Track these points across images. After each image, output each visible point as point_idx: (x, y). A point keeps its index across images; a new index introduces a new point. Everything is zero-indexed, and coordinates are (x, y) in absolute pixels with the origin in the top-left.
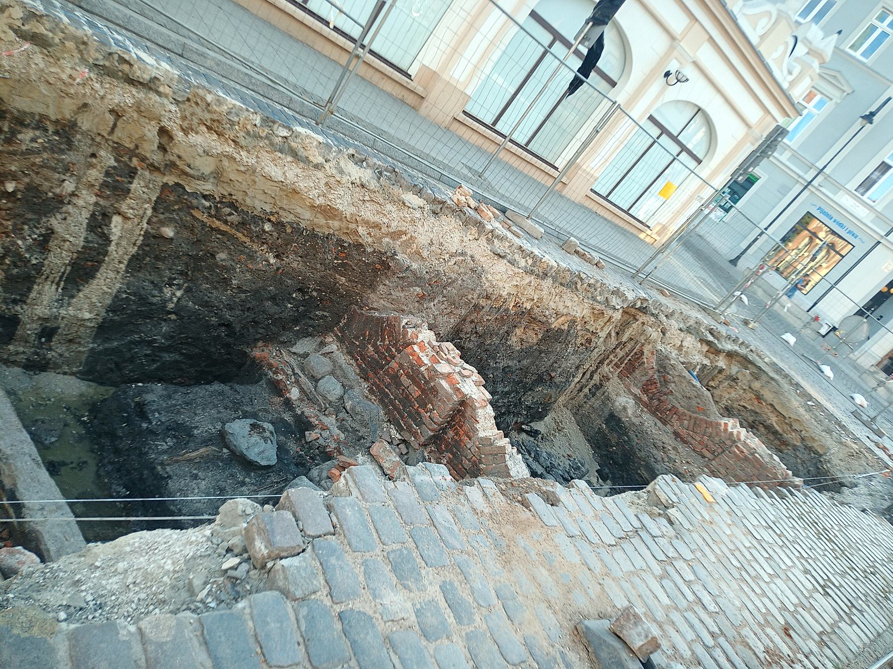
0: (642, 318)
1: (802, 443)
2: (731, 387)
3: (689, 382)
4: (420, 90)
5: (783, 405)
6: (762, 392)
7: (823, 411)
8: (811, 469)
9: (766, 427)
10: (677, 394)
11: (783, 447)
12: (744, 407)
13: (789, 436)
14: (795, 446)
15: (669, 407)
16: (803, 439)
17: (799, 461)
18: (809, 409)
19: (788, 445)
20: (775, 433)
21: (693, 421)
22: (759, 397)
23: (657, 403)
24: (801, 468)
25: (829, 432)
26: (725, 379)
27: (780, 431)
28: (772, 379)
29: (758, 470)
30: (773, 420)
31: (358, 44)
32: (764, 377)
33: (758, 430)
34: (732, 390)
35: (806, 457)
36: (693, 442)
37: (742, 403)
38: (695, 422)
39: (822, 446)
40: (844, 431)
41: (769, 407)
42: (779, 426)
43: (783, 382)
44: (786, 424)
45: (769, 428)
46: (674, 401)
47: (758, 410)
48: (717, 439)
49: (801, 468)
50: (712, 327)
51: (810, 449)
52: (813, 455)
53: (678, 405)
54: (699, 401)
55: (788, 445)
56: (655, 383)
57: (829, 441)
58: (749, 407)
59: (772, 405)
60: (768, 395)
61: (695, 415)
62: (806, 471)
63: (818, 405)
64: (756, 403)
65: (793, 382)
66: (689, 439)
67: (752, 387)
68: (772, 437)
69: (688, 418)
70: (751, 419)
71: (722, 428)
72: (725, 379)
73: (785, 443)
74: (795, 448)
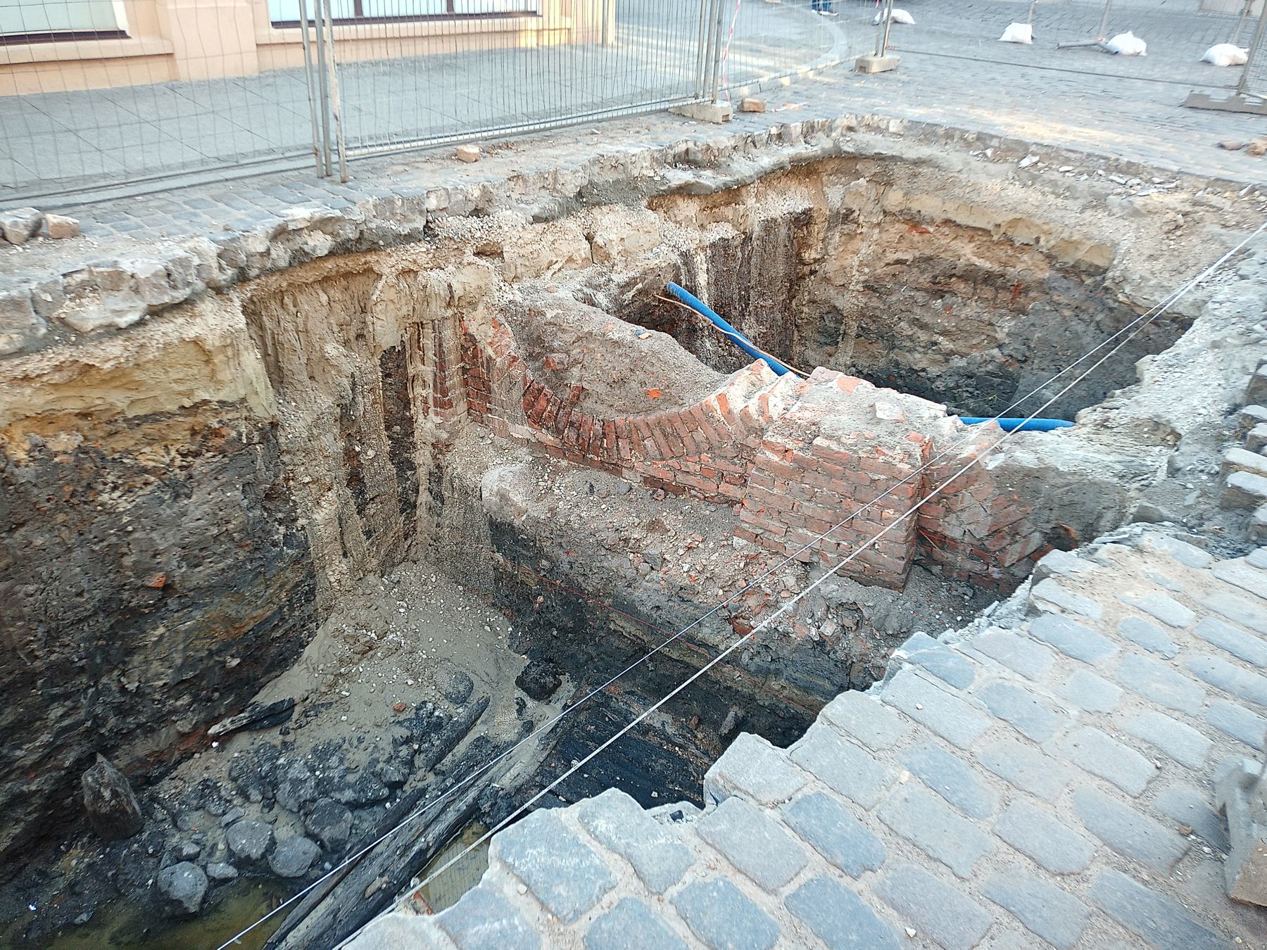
0: (387, 264)
1: (1052, 267)
2: (851, 236)
4: (152, 45)
5: (971, 207)
6: (915, 206)
7: (1067, 161)
8: (1099, 318)
11: (1022, 300)
12: (898, 262)
14: (1041, 283)
16: (1050, 257)
17: (1067, 313)
18: (1031, 178)
19: (1027, 290)
20: (988, 278)
21: (657, 432)
22: (915, 222)
23: (573, 435)
24: (1080, 328)
25: (1098, 202)
26: (829, 229)
27: (996, 268)
28: (918, 162)
29: (843, 477)
30: (968, 253)
31: (304, 24)
32: (899, 171)
34: (857, 244)
35: (1078, 293)
36: (691, 481)
37: (892, 257)
39: (1100, 247)
40: (1136, 175)
41: (946, 230)
42: (987, 259)
44: (998, 243)
45: (971, 276)
47: (928, 252)
48: (728, 446)
49: (1080, 328)
50: (683, 147)
51: (1074, 271)
52: (1089, 281)
55: (1027, 290)
56: (540, 391)
57: (1107, 226)
58: (908, 256)
59: (947, 222)
60: (929, 205)
61: (652, 418)
62: (1092, 328)
64: (916, 237)
65: (971, 137)
66: (680, 477)
67: (889, 208)
68: (988, 293)
69: (646, 433)
70: (924, 280)
71: (719, 414)
72: (829, 229)
73: (1020, 289)
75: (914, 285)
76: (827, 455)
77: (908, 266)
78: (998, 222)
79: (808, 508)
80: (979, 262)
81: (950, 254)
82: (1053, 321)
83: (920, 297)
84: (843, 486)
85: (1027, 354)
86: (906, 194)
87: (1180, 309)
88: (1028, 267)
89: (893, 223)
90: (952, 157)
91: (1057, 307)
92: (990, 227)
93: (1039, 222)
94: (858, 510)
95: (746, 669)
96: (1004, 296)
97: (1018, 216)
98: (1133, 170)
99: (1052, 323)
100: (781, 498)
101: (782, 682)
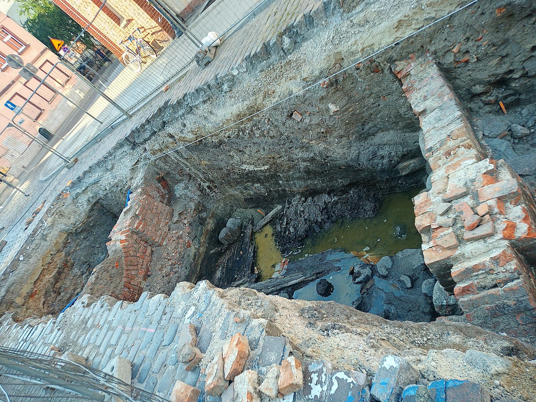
3: (95, 284)
6: (25, 294)
8: (82, 237)
9: (57, 282)
10: (111, 288)
12: (44, 304)
13: (58, 262)
14: (66, 256)
15: (126, 290)
16: (59, 251)
17: (78, 248)
18: (28, 256)
19: (67, 261)
20: (59, 273)
21: (130, 268)
22: (31, 295)
24: (83, 245)
25: (44, 237)
27: (56, 270)
28: (7, 291)
29: (147, 210)
30: (49, 277)
32: (9, 296)
33: (60, 288)
35: (72, 244)
36: (145, 263)
37: (41, 306)
38: (130, 265)
39: (60, 236)
43: (11, 278)
44: (48, 267)
45: (57, 279)
46: (119, 288)
47: (43, 292)
49: (83, 245)
51: (66, 244)
52: (69, 241)
53: (122, 283)
54: (111, 268)
55: (67, 261)
57: (55, 232)
58: (43, 300)
60: (26, 290)
61: (125, 267)
62: (84, 242)
63: (20, 253)
64: (36, 296)
66: (144, 267)
67: (22, 304)
68: (63, 275)
69: (129, 272)
70: (53, 295)
71: (126, 243)
73: (65, 264)
74: (68, 254)
75: (54, 299)
76: (141, 212)
77: (46, 300)
78: (41, 265)
79: (155, 222)
80: (53, 274)
81: (47, 284)
82: (79, 253)
83: (59, 298)
84: (149, 212)
85: (88, 264)
86: (19, 296)
87: (88, 209)
88: (59, 260)
89: (28, 303)
90: (11, 278)
91: (75, 251)
92: (42, 268)
93: (46, 252)
94: (154, 211)
95: (199, 247)
96: (66, 270)
97: (42, 259)
98: (35, 231)
99: (80, 253)
100: (152, 228)
101: (201, 239)
